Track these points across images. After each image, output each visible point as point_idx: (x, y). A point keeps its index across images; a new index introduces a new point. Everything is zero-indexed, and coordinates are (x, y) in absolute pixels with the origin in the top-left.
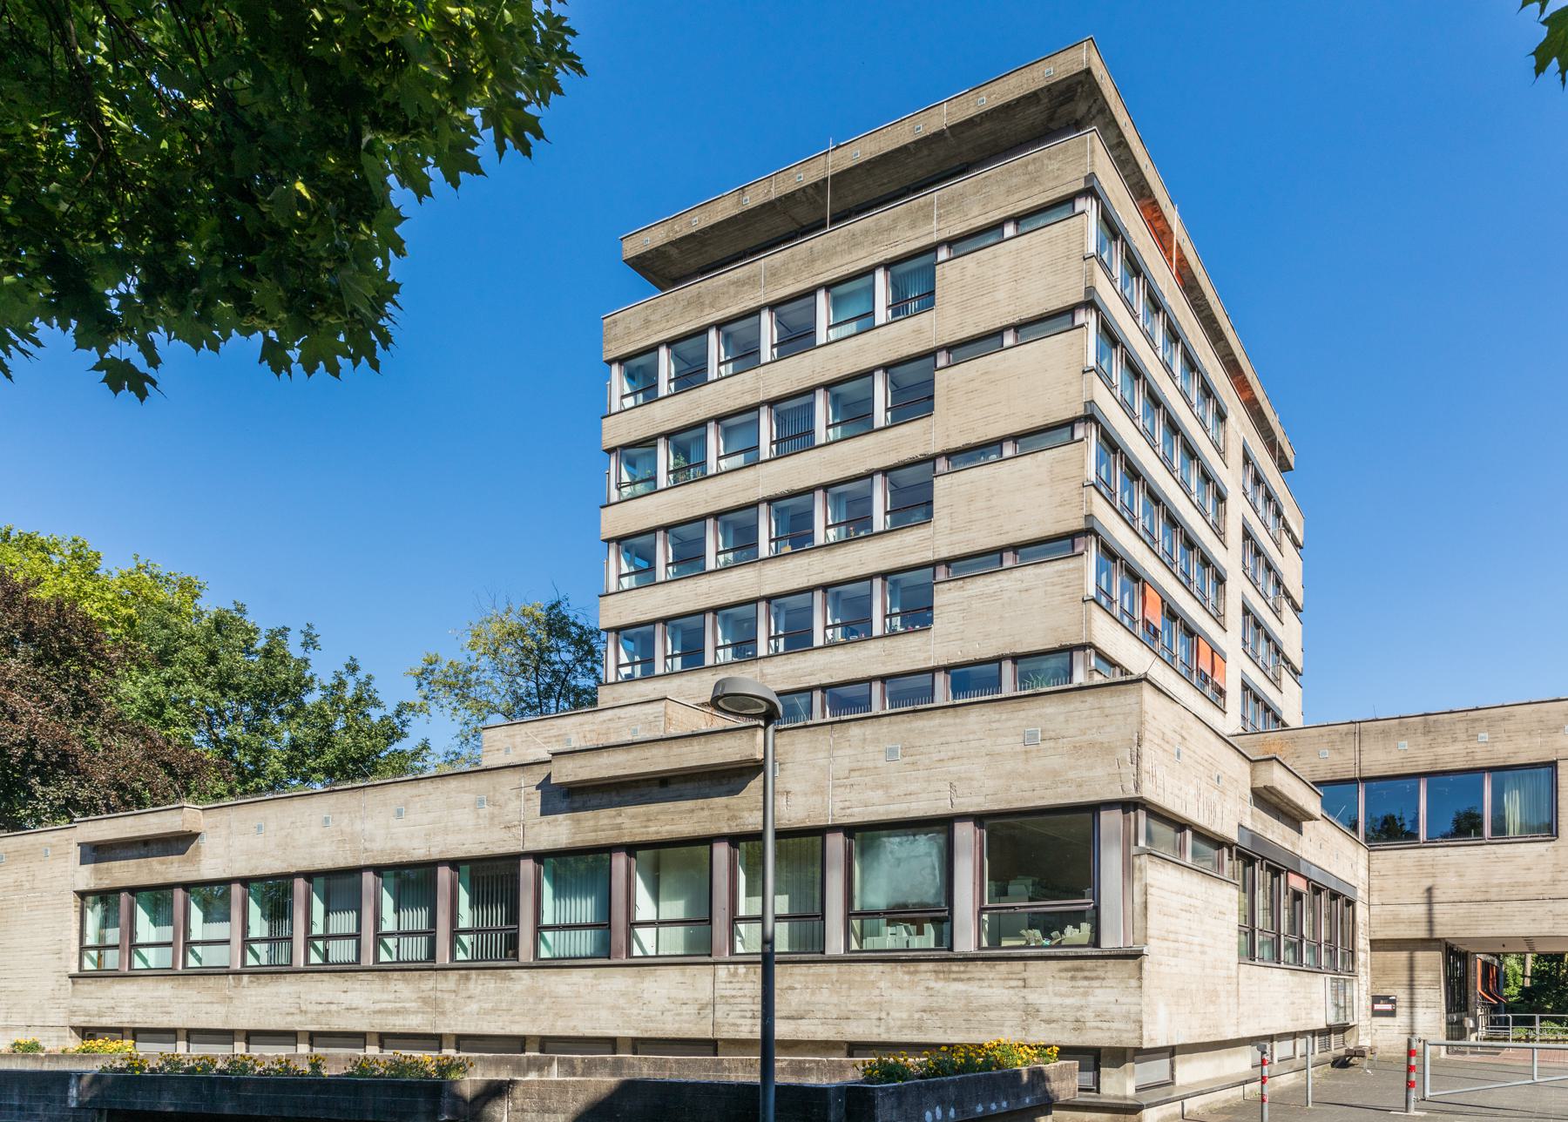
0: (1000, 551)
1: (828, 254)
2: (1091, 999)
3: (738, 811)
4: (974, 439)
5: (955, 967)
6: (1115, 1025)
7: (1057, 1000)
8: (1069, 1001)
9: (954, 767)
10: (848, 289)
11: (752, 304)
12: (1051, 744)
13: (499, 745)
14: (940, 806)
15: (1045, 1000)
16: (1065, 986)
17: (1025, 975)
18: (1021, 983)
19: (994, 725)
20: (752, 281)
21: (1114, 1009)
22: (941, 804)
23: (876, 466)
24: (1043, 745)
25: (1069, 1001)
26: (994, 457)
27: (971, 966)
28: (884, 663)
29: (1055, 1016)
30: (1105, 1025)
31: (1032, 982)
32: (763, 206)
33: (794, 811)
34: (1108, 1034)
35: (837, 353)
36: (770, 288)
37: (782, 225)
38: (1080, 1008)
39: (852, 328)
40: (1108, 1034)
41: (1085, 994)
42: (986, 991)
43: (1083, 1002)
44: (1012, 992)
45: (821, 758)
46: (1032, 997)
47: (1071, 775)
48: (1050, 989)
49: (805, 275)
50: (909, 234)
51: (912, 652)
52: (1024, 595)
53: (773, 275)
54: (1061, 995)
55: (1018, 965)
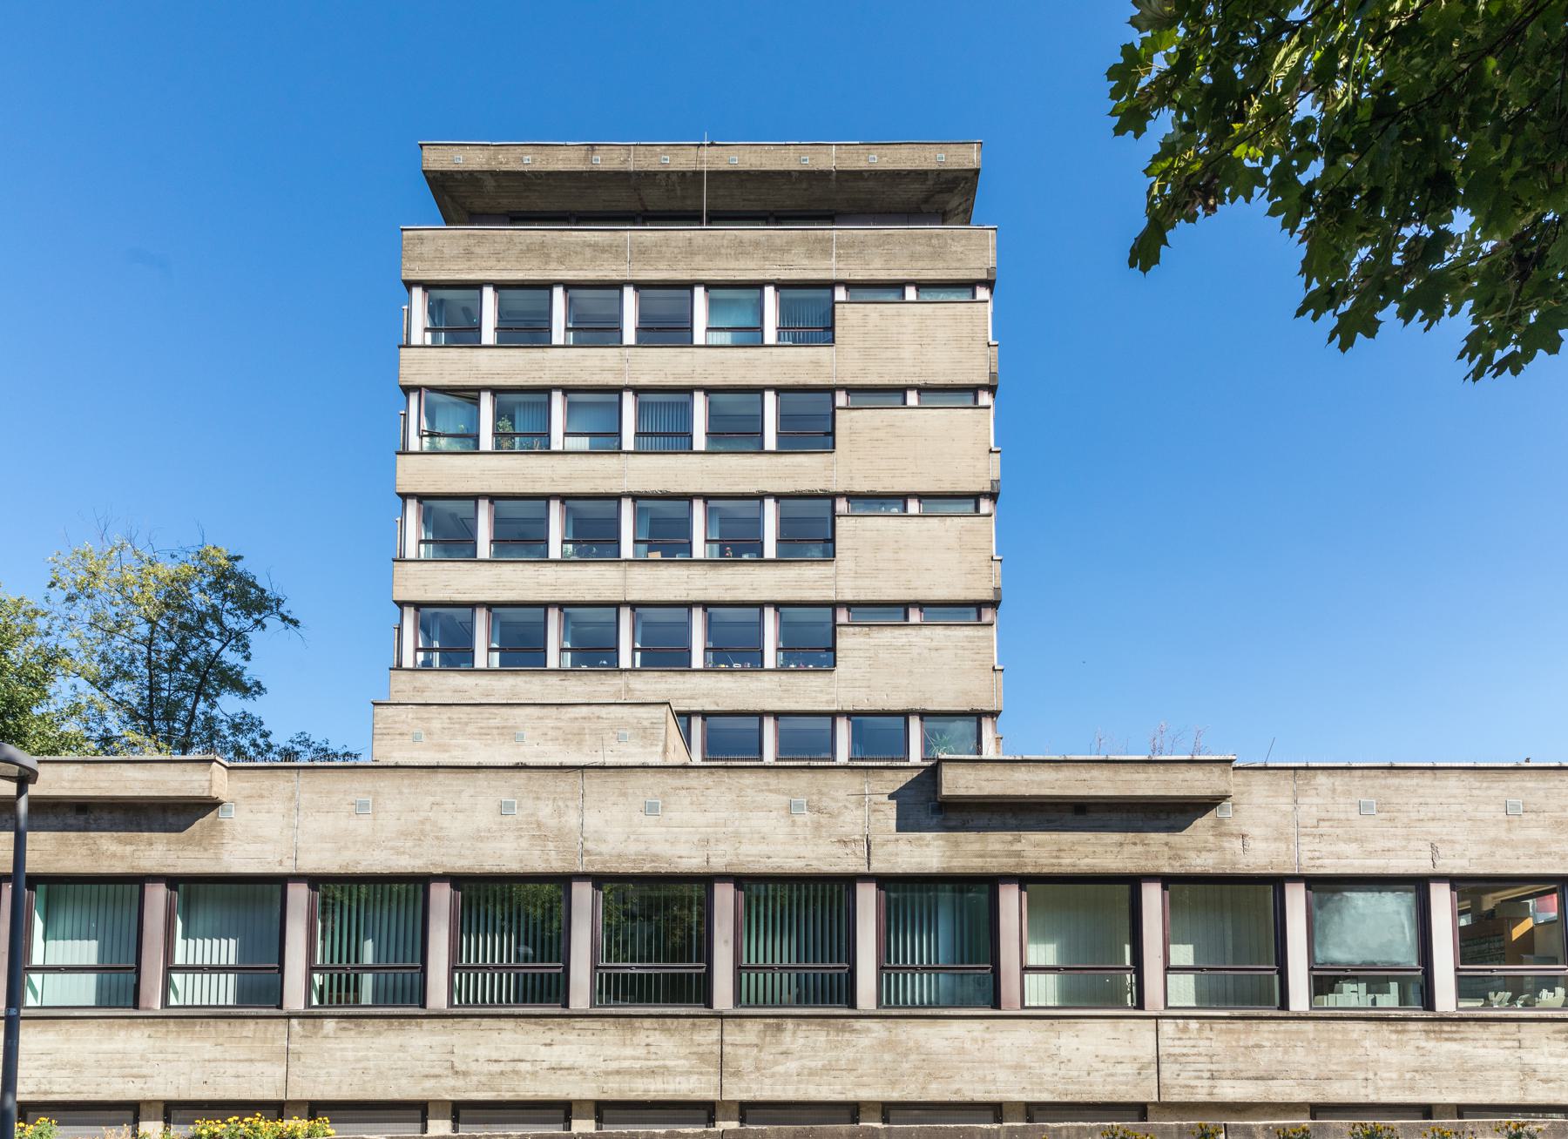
0: (906, 605)
1: (713, 253)
3: (1197, 850)
4: (879, 488)
9: (1434, 827)
10: (736, 293)
11: (614, 276)
12: (1533, 816)
13: (404, 728)
14: (1417, 864)
19: (1475, 792)
20: (616, 252)
22: (1423, 863)
23: (770, 490)
24: (1526, 816)
26: (895, 510)
28: (780, 699)
32: (617, 173)
33: (1258, 857)
35: (707, 360)
36: (638, 266)
37: (623, 199)
39: (726, 338)
45: (1284, 803)
47: (1554, 848)
49: (682, 265)
50: (805, 262)
51: (808, 692)
52: (934, 654)
53: (641, 252)
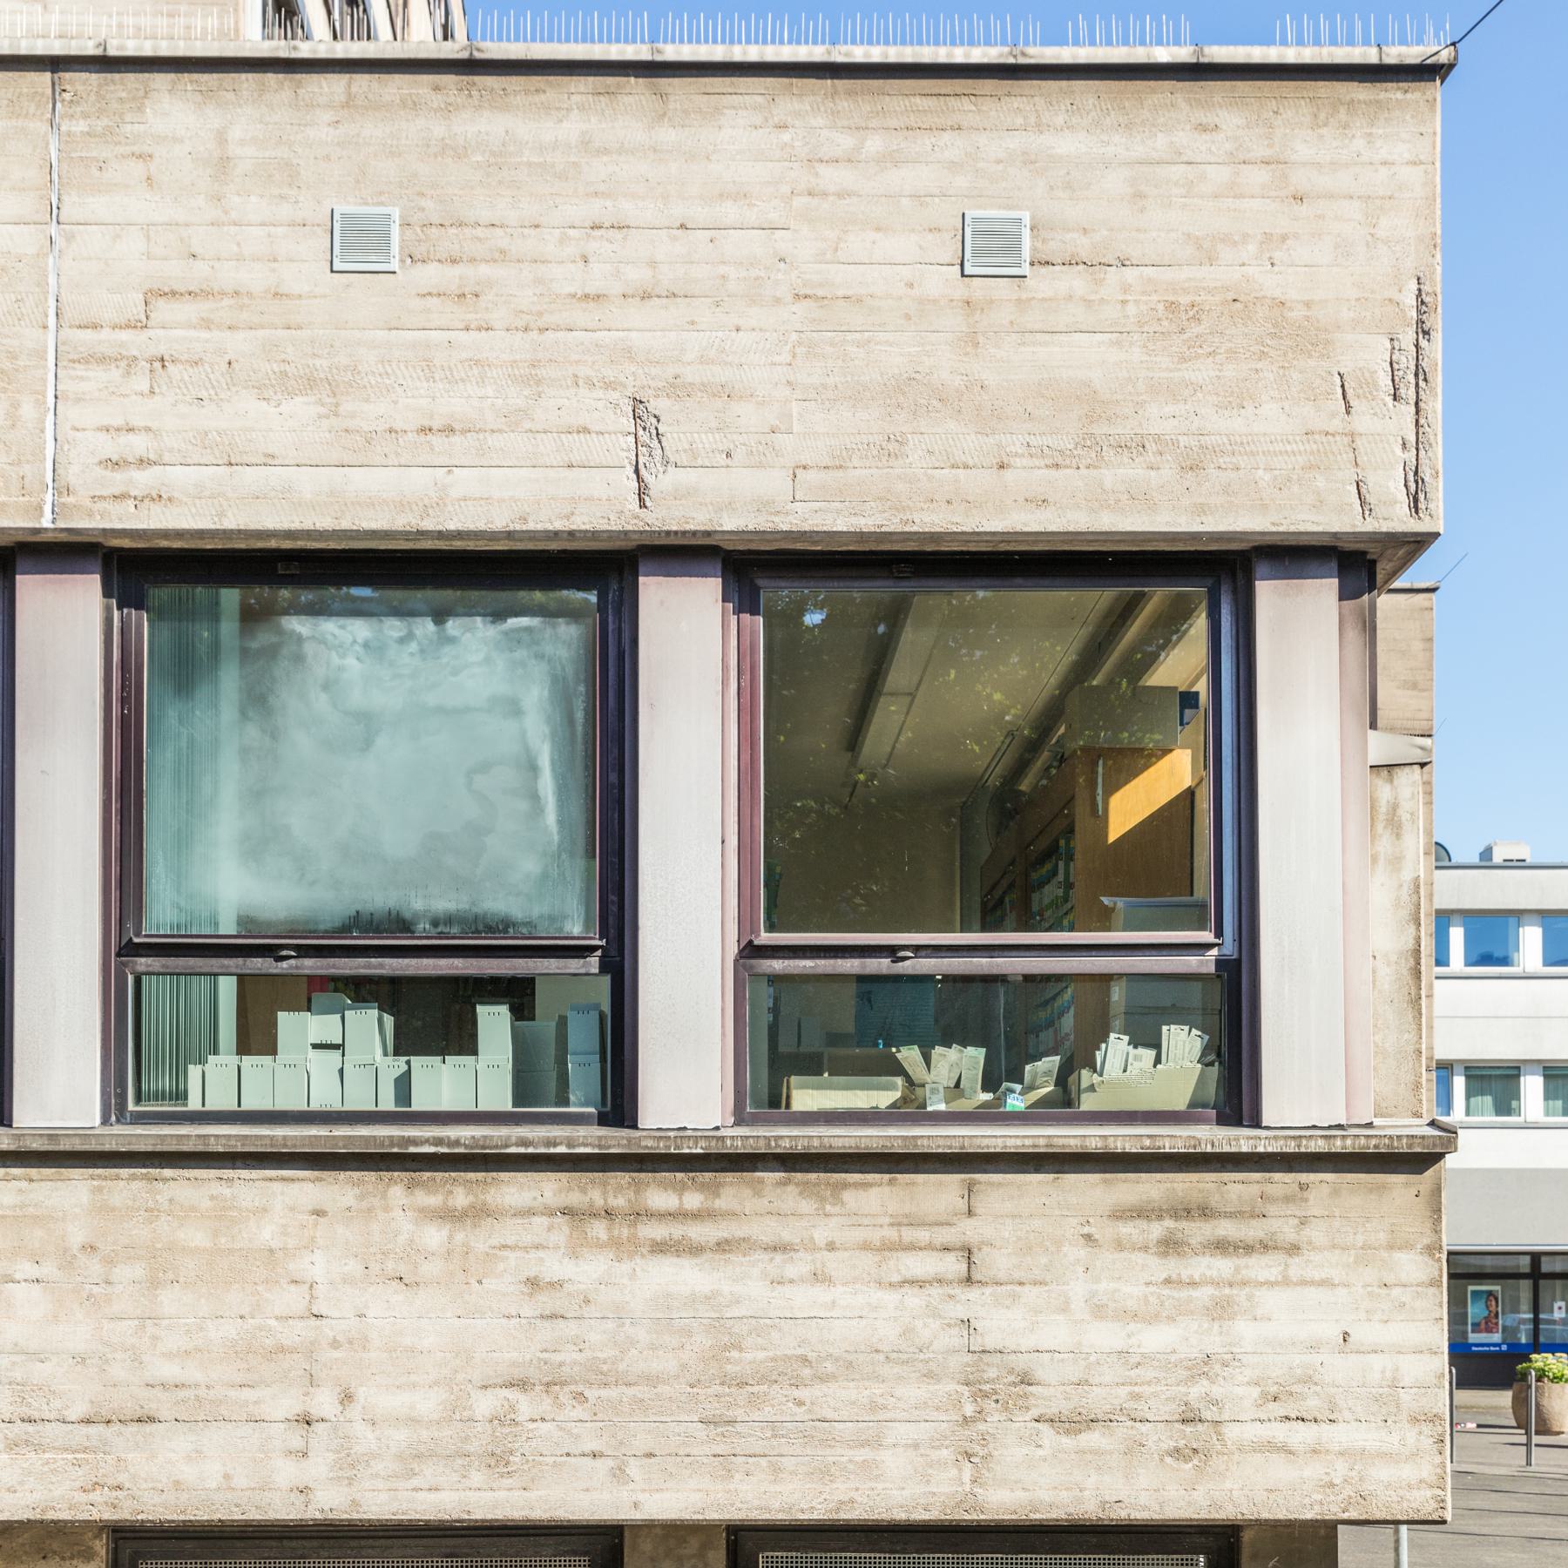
2: (1244, 1329)
5: (660, 1194)
6: (1340, 1435)
7: (1105, 1337)
8: (1155, 1339)
15: (1056, 1333)
16: (1136, 1275)
17: (969, 1230)
18: (953, 1265)
21: (1338, 1368)
25: (1155, 1339)
27: (733, 1191)
29: (1097, 1400)
30: (1301, 1435)
31: (997, 1262)
34: (1313, 1471)
38: (1203, 1366)
40: (1313, 1471)
41: (1221, 1311)
42: (804, 1298)
43: (1213, 1342)
44: (914, 1299)
46: (1003, 1322)
48: (1078, 1289)
54: (1128, 1316)
55: (942, 1191)
